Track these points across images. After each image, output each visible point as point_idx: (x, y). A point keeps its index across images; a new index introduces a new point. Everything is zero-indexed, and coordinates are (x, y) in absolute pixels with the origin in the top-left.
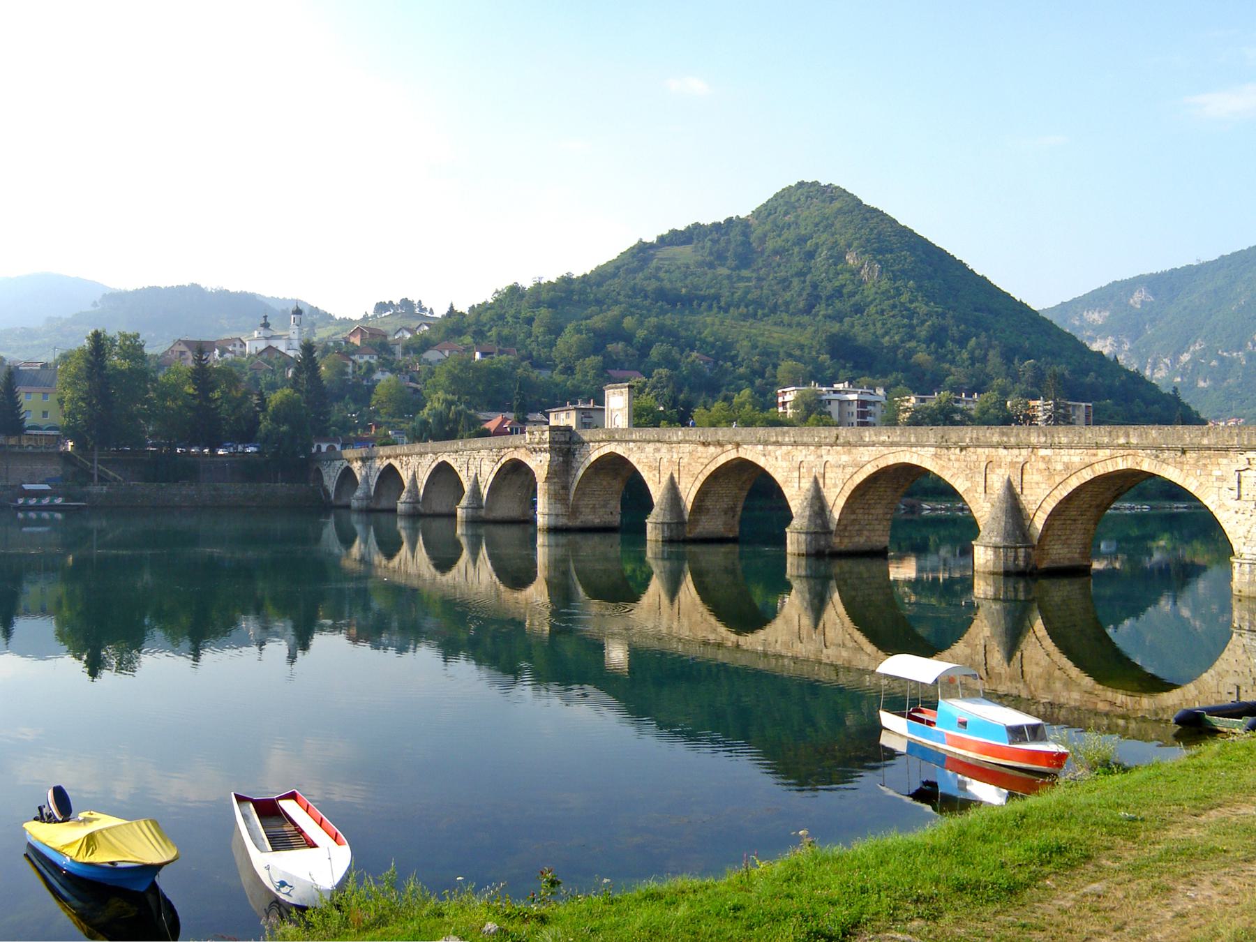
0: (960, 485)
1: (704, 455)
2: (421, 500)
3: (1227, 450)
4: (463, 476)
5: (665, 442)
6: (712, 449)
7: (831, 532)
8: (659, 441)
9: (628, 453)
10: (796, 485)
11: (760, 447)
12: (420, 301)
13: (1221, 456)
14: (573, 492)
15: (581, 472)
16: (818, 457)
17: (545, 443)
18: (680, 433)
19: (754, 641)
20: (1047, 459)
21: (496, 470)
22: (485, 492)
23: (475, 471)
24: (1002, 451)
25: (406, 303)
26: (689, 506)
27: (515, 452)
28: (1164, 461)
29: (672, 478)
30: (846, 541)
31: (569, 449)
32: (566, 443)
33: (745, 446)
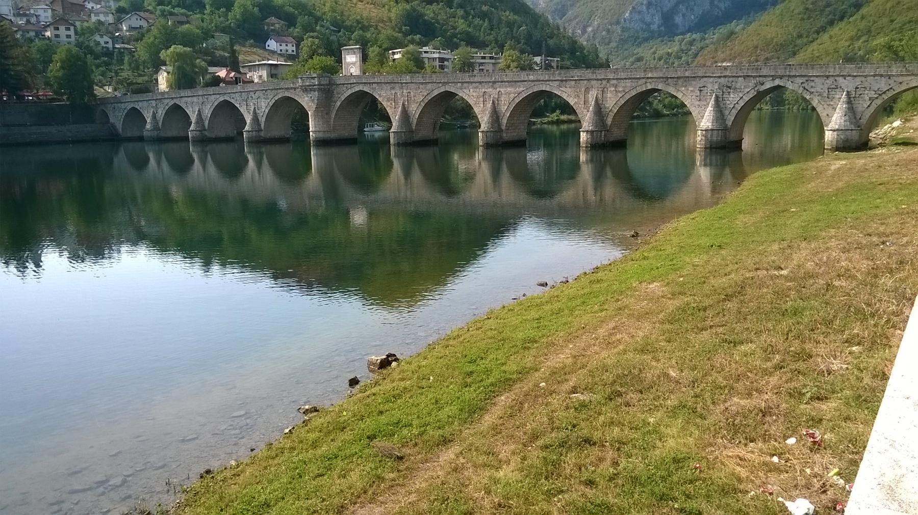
0: (572, 101)
4: (243, 110)
6: (429, 86)
7: (502, 131)
9: (372, 91)
10: (482, 105)
13: (693, 80)
15: (338, 104)
17: (315, 85)
19: (454, 200)
21: (271, 104)
22: (263, 120)
24: (595, 81)
26: (415, 121)
28: (668, 84)
29: (403, 105)
30: (509, 135)
32: (328, 85)
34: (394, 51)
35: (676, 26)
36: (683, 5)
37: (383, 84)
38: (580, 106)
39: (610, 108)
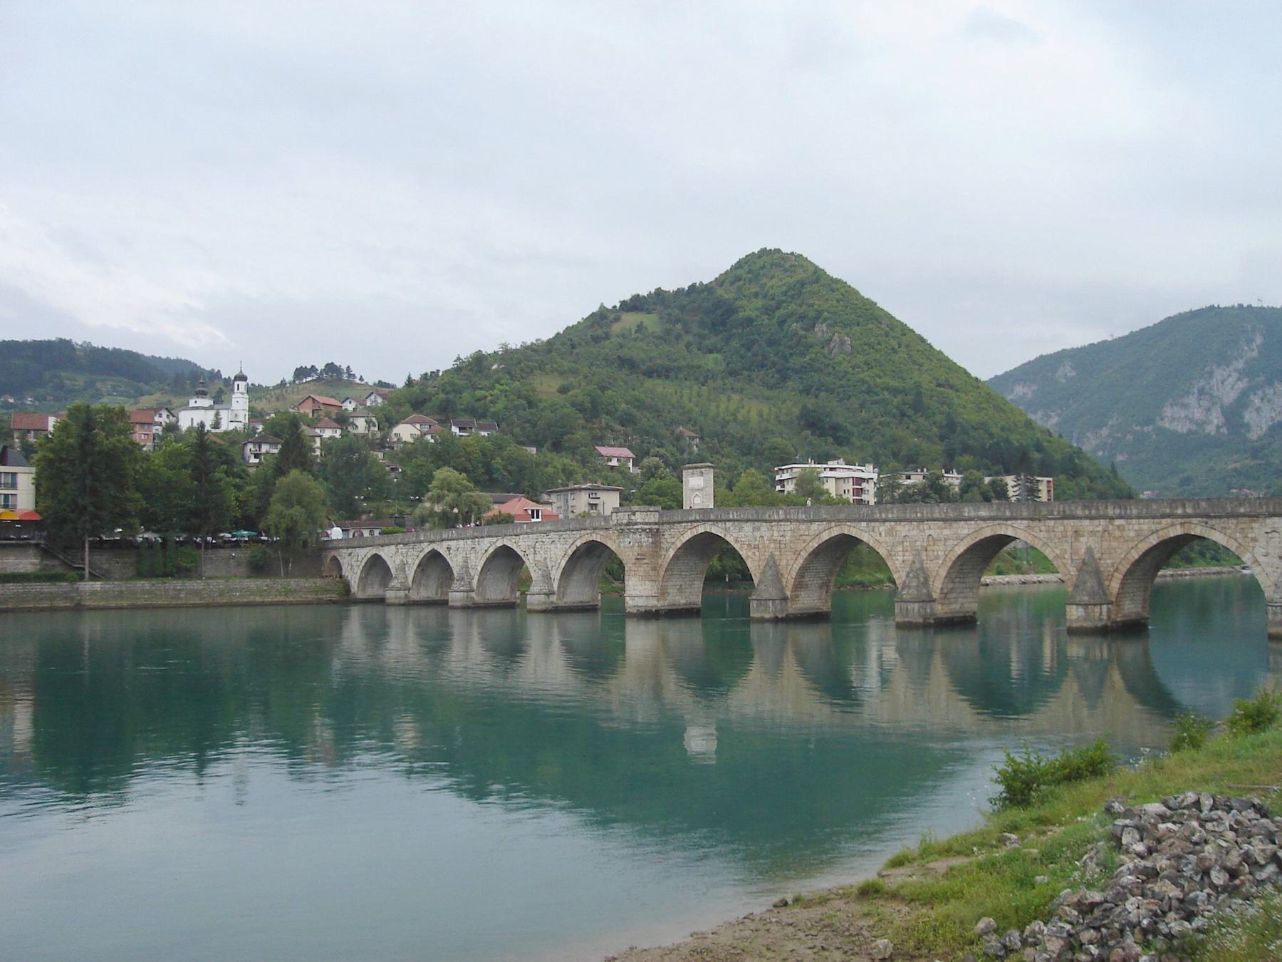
1: (807, 533)
2: (475, 587)
3: (1258, 516)
5: (766, 521)
6: (815, 526)
8: (757, 521)
11: (864, 524)
12: (349, 367)
13: (1254, 521)
14: (662, 573)
15: (671, 553)
16: (921, 531)
17: (636, 524)
18: (781, 512)
20: (1121, 528)
21: (570, 552)
23: (544, 556)
24: (1087, 522)
25: (331, 367)
27: (594, 535)
31: (658, 530)
32: (656, 524)
33: (848, 524)
34: (783, 467)
35: (1247, 427)
36: (1255, 394)
37: (744, 525)
38: (1065, 561)
39: (1116, 565)
